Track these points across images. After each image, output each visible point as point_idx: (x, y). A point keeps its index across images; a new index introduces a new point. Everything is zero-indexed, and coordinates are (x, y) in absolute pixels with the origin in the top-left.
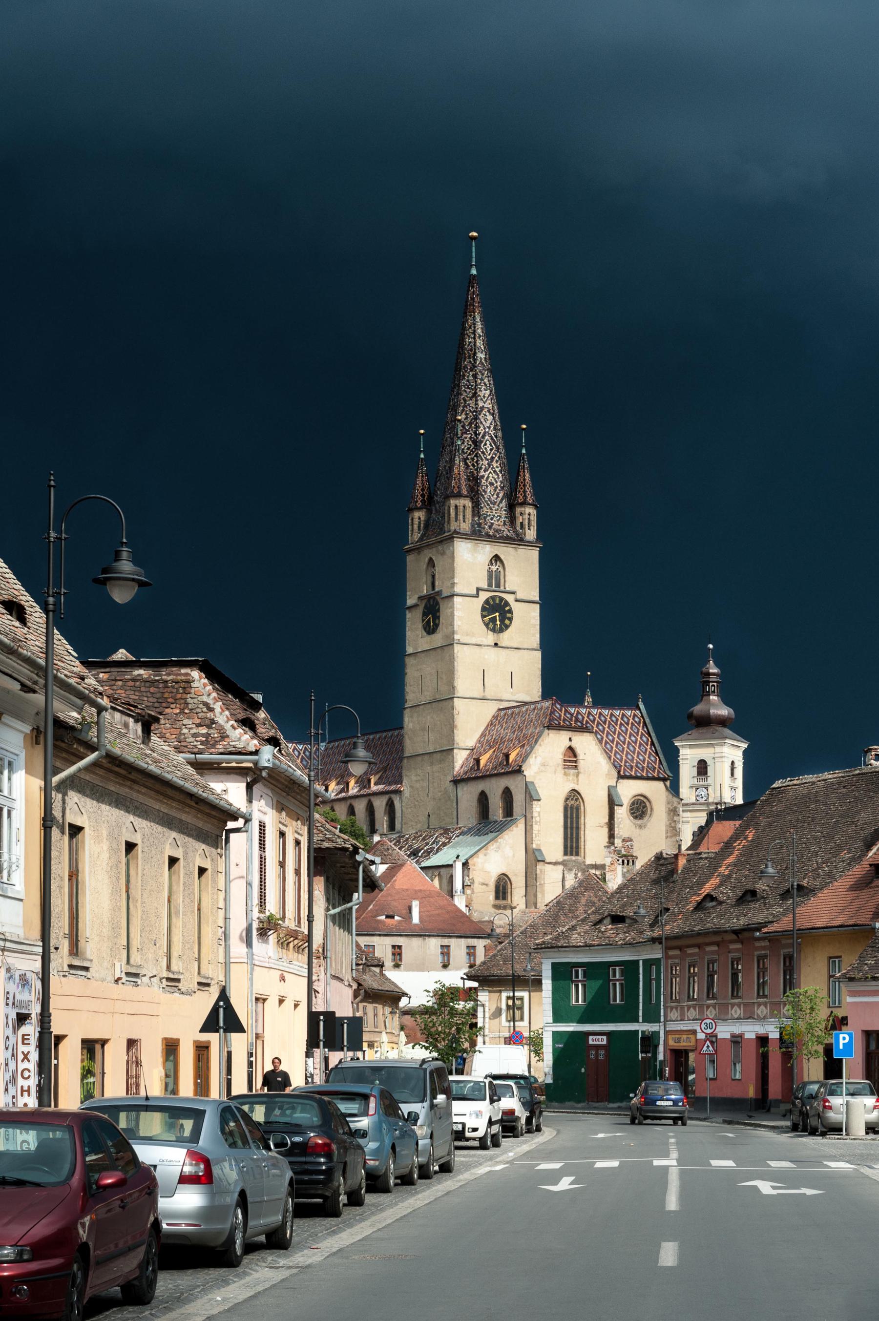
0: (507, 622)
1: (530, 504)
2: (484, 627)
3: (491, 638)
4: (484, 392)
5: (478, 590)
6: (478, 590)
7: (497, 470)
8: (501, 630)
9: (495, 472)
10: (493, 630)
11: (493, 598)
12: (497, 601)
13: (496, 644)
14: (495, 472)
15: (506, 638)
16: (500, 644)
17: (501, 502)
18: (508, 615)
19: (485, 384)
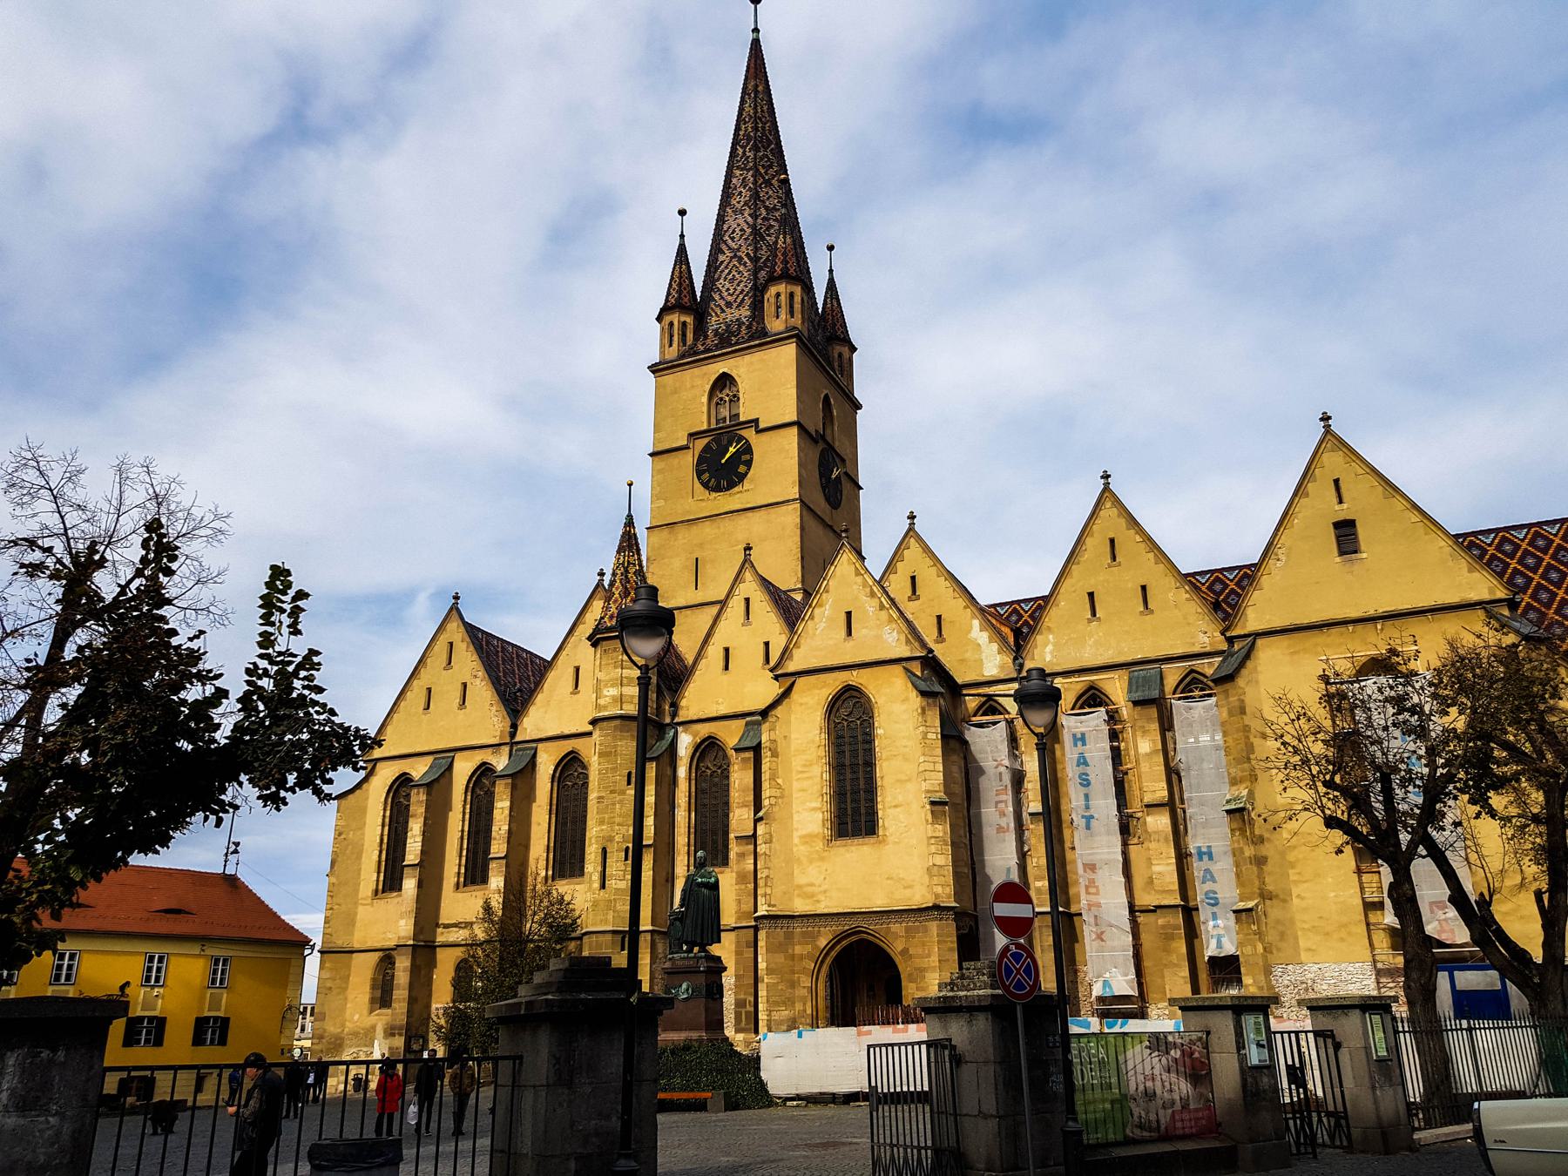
0: (742, 469)
6: (693, 436)
8: (731, 485)
18: (748, 457)
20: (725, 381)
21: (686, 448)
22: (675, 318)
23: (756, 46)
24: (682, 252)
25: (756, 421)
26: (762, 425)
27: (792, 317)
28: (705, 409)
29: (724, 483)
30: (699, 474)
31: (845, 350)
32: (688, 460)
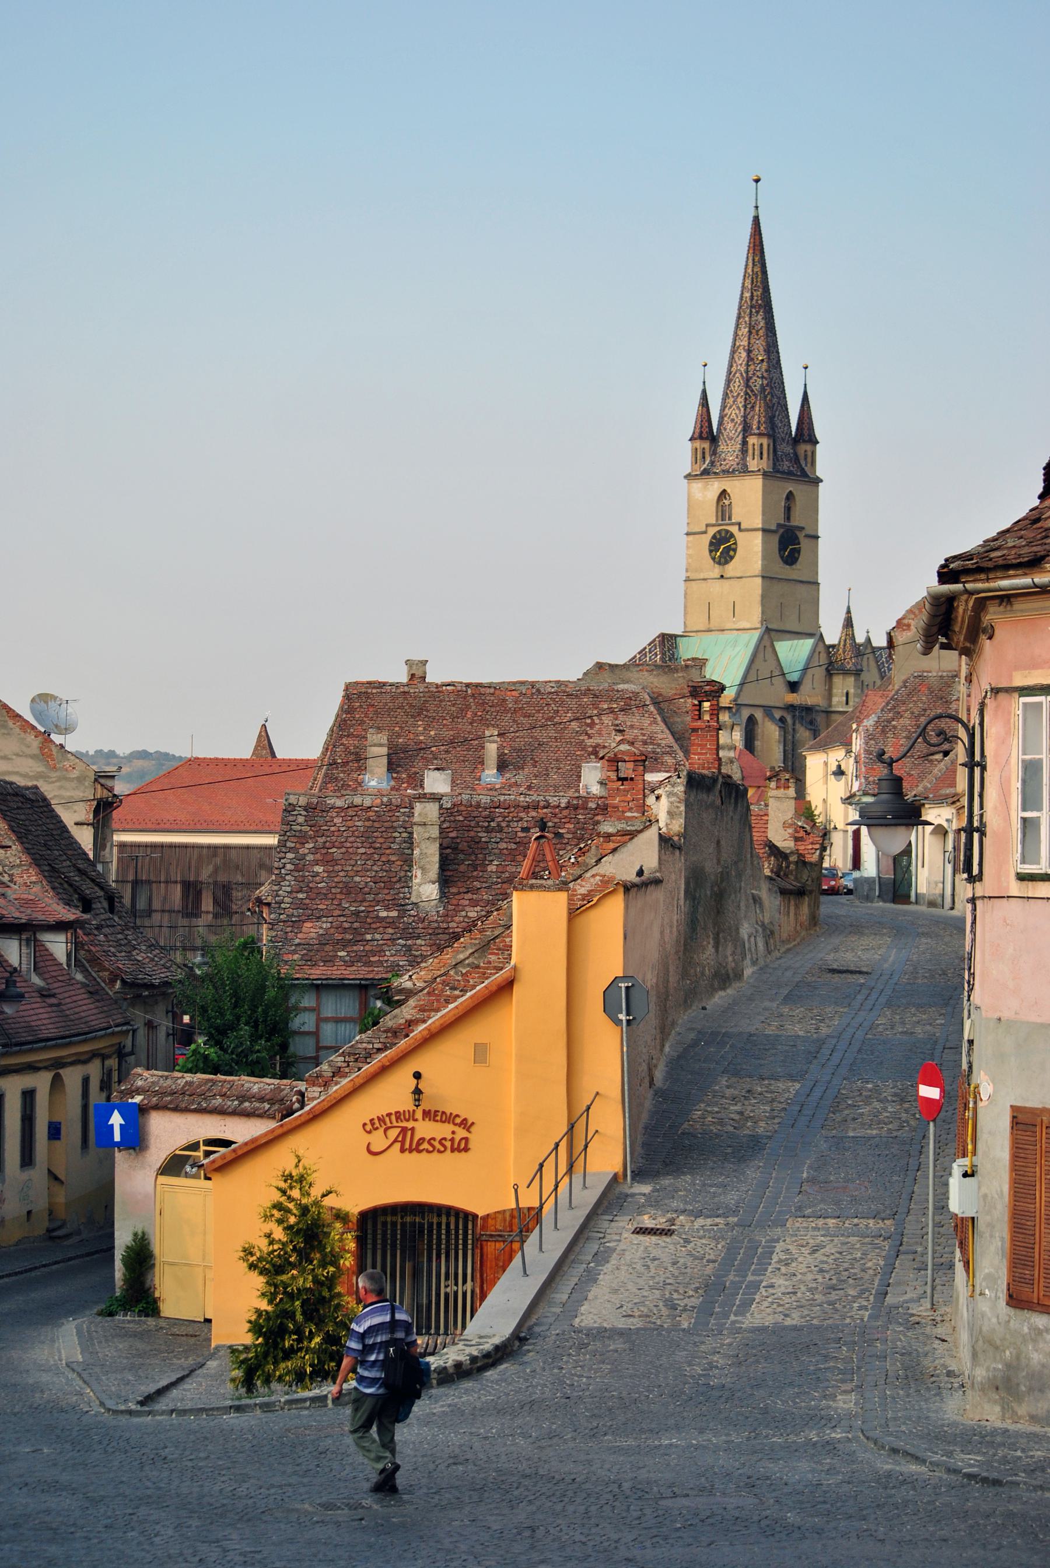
0: (732, 553)
1: (755, 434)
2: (711, 561)
3: (717, 571)
4: (743, 329)
5: (707, 525)
6: (707, 525)
7: (740, 405)
8: (726, 562)
9: (738, 408)
10: (719, 563)
11: (719, 532)
12: (723, 535)
13: (722, 576)
14: (738, 408)
15: (731, 569)
16: (725, 576)
17: (738, 437)
19: (746, 322)
20: (724, 494)
21: (705, 532)
22: (698, 444)
23: (756, 221)
24: (704, 392)
25: (739, 524)
26: (742, 527)
27: (761, 458)
28: (714, 509)
29: (723, 560)
30: (711, 551)
31: (808, 447)
32: (706, 539)
